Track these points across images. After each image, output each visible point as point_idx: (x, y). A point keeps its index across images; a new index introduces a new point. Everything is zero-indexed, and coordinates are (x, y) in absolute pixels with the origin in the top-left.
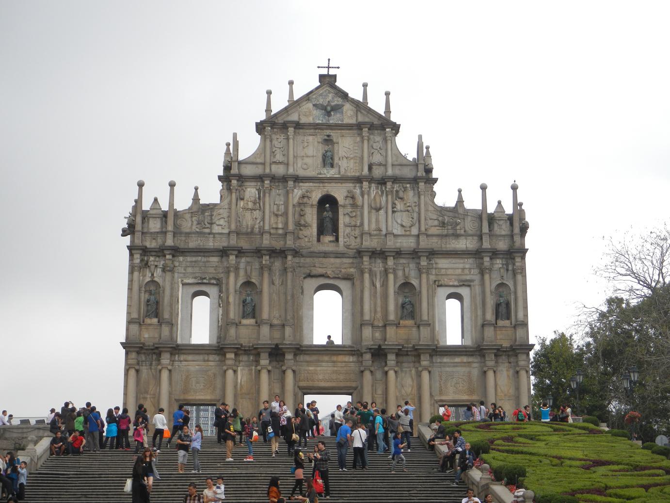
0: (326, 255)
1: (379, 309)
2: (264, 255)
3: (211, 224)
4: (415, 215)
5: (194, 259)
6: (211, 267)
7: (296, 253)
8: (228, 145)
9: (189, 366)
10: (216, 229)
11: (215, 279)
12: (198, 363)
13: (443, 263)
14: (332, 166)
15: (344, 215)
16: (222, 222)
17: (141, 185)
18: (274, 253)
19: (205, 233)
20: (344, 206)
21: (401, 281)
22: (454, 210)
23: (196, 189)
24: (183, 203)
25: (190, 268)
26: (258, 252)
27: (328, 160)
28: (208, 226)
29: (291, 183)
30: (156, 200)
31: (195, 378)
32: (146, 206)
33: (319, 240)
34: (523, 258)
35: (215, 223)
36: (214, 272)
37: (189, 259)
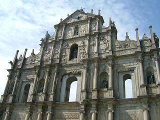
0: (71, 65)
1: (91, 85)
3: (35, 60)
4: (107, 45)
7: (60, 65)
10: (36, 62)
13: (120, 62)
14: (77, 34)
17: (18, 51)
18: (52, 66)
20: (80, 47)
21: (101, 71)
22: (126, 41)
23: (33, 50)
24: (28, 55)
26: (46, 67)
27: (76, 32)
29: (61, 43)
32: (18, 58)
33: (70, 60)
34: (158, 54)
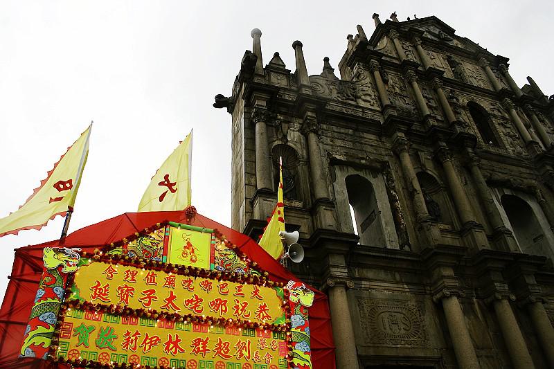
2: (440, 140)
3: (357, 97)
5: (342, 131)
6: (368, 145)
8: (350, 37)
9: (374, 289)
11: (377, 161)
12: (386, 285)
15: (499, 124)
16: (368, 98)
19: (351, 105)
20: (495, 116)
24: (314, 68)
25: (339, 141)
28: (352, 97)
30: (277, 55)
31: (388, 314)
35: (360, 98)
36: (375, 152)
37: (335, 128)
